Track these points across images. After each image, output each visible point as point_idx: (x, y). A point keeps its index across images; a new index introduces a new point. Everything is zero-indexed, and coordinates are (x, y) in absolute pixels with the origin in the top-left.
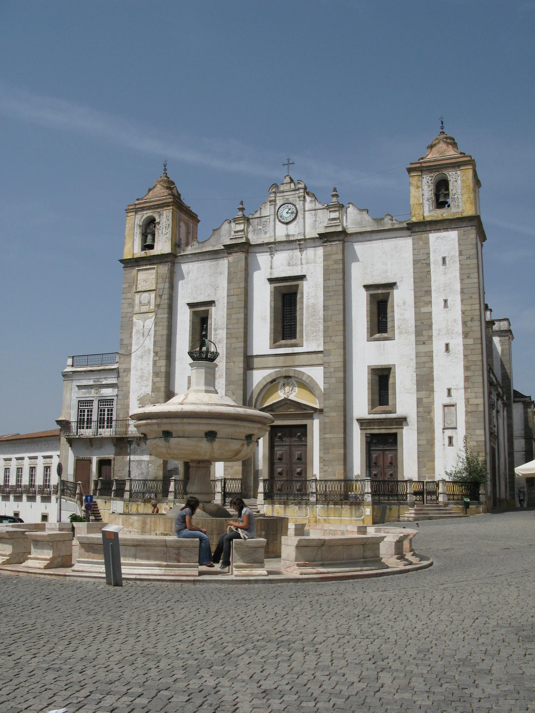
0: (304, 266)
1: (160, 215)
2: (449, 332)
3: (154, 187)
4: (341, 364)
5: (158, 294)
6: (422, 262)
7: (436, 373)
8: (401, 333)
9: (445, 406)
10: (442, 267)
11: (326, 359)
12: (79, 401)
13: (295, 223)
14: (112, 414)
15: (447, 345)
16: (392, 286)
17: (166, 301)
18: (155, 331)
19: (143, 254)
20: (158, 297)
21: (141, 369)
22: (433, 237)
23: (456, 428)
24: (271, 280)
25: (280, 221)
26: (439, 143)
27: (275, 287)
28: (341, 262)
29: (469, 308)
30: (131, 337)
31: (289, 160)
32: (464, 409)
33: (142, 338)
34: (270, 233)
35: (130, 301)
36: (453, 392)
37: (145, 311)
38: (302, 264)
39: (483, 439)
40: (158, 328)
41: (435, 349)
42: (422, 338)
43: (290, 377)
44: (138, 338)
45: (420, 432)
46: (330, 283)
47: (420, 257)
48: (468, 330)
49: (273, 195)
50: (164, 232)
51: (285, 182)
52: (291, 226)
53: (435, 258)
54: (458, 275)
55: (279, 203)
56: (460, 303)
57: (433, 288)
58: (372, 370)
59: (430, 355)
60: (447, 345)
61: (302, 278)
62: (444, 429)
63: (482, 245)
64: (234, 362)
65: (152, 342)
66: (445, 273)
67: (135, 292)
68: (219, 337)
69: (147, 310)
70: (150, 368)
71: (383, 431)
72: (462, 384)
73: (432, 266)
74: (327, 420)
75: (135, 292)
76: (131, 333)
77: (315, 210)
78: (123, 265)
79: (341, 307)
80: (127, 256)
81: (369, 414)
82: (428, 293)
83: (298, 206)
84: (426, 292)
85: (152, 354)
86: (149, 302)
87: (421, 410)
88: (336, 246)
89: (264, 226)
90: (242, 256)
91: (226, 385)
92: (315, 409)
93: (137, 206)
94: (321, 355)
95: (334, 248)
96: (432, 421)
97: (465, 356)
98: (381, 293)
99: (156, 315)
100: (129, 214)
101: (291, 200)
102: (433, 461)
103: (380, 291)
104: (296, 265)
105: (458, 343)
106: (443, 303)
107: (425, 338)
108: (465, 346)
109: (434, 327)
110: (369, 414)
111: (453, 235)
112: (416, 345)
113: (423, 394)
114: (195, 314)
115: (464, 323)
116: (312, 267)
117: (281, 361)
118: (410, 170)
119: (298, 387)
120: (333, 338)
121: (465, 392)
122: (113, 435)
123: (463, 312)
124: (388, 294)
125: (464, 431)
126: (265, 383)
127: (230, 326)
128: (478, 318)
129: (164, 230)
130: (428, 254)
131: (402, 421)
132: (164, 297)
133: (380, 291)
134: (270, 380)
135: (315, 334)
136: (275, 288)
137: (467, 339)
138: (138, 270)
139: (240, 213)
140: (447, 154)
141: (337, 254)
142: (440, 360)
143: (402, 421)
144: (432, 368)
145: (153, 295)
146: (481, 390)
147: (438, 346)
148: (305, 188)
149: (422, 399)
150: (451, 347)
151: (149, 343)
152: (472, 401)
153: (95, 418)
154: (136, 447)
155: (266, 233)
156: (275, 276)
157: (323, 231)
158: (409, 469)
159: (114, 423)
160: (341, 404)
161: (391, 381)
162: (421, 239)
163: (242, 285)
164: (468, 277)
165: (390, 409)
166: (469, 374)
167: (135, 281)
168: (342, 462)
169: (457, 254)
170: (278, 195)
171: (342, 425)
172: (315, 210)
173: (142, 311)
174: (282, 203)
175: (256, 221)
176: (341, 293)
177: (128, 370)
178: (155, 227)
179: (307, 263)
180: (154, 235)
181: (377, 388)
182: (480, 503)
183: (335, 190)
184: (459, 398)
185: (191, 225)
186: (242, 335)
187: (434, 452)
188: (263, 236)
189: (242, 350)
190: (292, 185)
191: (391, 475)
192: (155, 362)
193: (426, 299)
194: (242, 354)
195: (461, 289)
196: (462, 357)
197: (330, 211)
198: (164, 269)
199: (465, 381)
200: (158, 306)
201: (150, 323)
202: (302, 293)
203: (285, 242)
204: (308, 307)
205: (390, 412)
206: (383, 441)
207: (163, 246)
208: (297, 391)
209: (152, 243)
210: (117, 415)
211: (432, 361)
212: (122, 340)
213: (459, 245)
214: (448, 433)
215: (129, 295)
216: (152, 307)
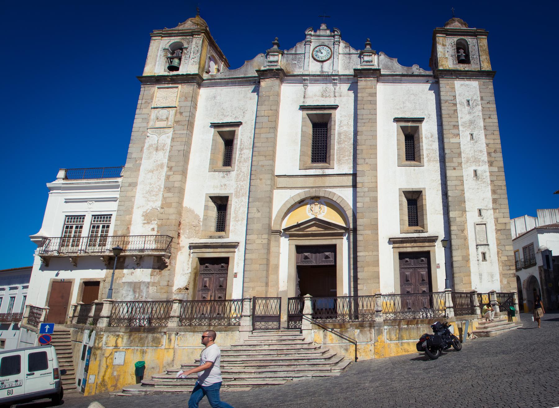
2: (476, 160)
5: (179, 111)
6: (450, 102)
7: (467, 195)
10: (466, 107)
15: (475, 171)
16: (420, 120)
29: (492, 142)
36: (483, 213)
41: (465, 174)
48: (493, 159)
54: (481, 114)
56: (484, 137)
57: (460, 123)
59: (461, 179)
60: (475, 171)
67: (152, 108)
69: (165, 126)
71: (416, 250)
72: (491, 205)
73: (458, 106)
75: (152, 108)
82: (456, 127)
84: (454, 126)
86: (167, 118)
98: (411, 126)
99: (174, 131)
103: (410, 124)
105: (484, 169)
106: (469, 136)
109: (463, 155)
111: (474, 84)
115: (489, 154)
117: (310, 182)
121: (494, 213)
123: (487, 145)
124: (417, 129)
126: (293, 203)
130: (455, 97)
132: (184, 114)
133: (410, 124)
135: (347, 158)
137: (492, 168)
138: (159, 88)
142: (469, 183)
144: (463, 190)
145: (172, 112)
147: (467, 172)
150: (478, 173)
152: (501, 220)
162: (448, 84)
164: (489, 118)
166: (496, 196)
169: (479, 99)
184: (489, 217)
193: (455, 131)
195: (484, 126)
196: (489, 182)
199: (493, 203)
200: (177, 122)
201: (166, 138)
204: (340, 134)
208: (326, 212)
211: (463, 184)
213: (480, 92)
215: (145, 111)
216: (170, 123)
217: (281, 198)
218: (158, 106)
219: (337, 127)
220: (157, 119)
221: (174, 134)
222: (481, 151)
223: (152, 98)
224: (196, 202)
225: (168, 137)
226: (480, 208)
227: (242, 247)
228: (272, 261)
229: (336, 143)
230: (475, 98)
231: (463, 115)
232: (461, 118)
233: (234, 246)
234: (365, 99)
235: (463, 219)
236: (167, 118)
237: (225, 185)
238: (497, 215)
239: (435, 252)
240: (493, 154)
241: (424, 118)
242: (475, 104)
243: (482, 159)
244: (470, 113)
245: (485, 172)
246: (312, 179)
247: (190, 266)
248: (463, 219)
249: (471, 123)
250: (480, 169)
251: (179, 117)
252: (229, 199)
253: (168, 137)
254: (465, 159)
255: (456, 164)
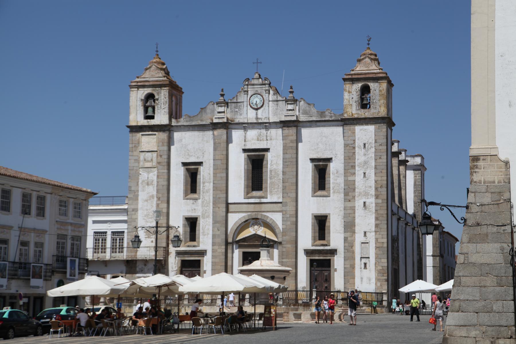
0: (269, 142)
1: (158, 94)
2: (366, 194)
3: (150, 67)
4: (294, 212)
7: (357, 221)
8: (334, 192)
9: (362, 243)
10: (363, 150)
11: (284, 208)
12: (94, 232)
13: (262, 109)
14: (123, 242)
16: (329, 160)
17: (166, 160)
18: (158, 182)
19: (145, 122)
20: (159, 156)
21: (147, 210)
22: (358, 129)
23: (369, 258)
24: (245, 151)
25: (251, 107)
26: (365, 58)
27: (248, 155)
28: (295, 142)
29: (379, 179)
30: (138, 185)
31: (257, 60)
32: (374, 245)
33: (147, 186)
34: (244, 115)
35: (136, 158)
36: (367, 234)
37: (149, 166)
38: (267, 140)
39: (386, 265)
40: (160, 180)
42: (349, 198)
43: (258, 219)
44: (144, 187)
45: (345, 259)
46: (287, 156)
47: (349, 142)
48: (379, 193)
49: (246, 87)
50: (162, 107)
51: (255, 77)
52: (260, 111)
53: (359, 143)
54: (373, 156)
55: (250, 93)
58: (315, 216)
59: (353, 209)
60: (365, 203)
61: (267, 150)
62: (361, 258)
63: (392, 130)
64: (219, 208)
65: (155, 190)
66: (365, 155)
68: (206, 188)
69: (151, 166)
70: (155, 209)
71: (321, 258)
72: (373, 229)
73: (357, 149)
74: (284, 250)
76: (138, 182)
77: (277, 101)
78: (129, 129)
79: (295, 173)
80: (133, 123)
81: (312, 246)
82: (353, 167)
83: (264, 97)
84: (352, 166)
85: (155, 199)
86: (152, 160)
87: (347, 244)
88: (292, 131)
89: (240, 109)
90: (224, 131)
91: (213, 224)
92: (275, 242)
93: (139, 84)
94: (280, 205)
95: (291, 131)
96: (353, 252)
97: (376, 210)
98: (322, 165)
100: (132, 89)
101: (259, 92)
102: (354, 278)
104: (263, 140)
105: (371, 201)
106: (363, 174)
107: (351, 197)
108: (376, 204)
109: (357, 190)
110: (312, 246)
111: (371, 128)
112: (344, 201)
113: (348, 234)
114: (188, 170)
115: (376, 189)
116: (274, 142)
117: (251, 208)
118: (345, 80)
119: (264, 227)
120: (289, 194)
121: (375, 234)
122: (125, 258)
123: (376, 182)
124: (326, 166)
125: (374, 259)
127: (215, 182)
128: (386, 186)
129: (162, 105)
131: (333, 252)
132: (163, 156)
134: (244, 220)
135: (276, 190)
136: (248, 155)
138: (142, 135)
139: (222, 98)
140: (370, 68)
141: (292, 135)
143: (333, 252)
144: (355, 217)
145: (155, 154)
146: (386, 233)
147: (359, 204)
148: (270, 84)
149: (347, 238)
150: (367, 204)
151: (152, 190)
152: (379, 240)
153: (109, 244)
154: (144, 266)
155: (241, 115)
156: (247, 147)
157: (283, 119)
158: (338, 283)
159: (125, 250)
160: (295, 239)
161: (327, 224)
162: (350, 130)
163: (225, 153)
164: (380, 158)
165: (326, 243)
166: (378, 222)
167: (139, 142)
168: (294, 278)
169: (374, 141)
170: (249, 87)
171: (295, 253)
172: (277, 101)
173: (146, 166)
174: (253, 93)
175: (233, 105)
176: (295, 163)
177: (136, 210)
178: (154, 101)
179: (271, 139)
180: (154, 108)
181: (317, 228)
182: (383, 307)
183: (291, 88)
184: (372, 238)
185: (179, 97)
186: (225, 188)
187: (354, 272)
188: (239, 117)
189: (225, 200)
190: (260, 80)
191: (326, 287)
192: (158, 205)
193: (352, 171)
194: (225, 202)
195: (375, 166)
196: (374, 211)
197: (288, 104)
198: (163, 136)
199: (375, 227)
200: (159, 163)
201: (153, 175)
202: (267, 161)
203: (255, 123)
204: (271, 171)
205: (326, 245)
206: (321, 264)
207: (161, 117)
209: (153, 115)
210: (128, 243)
211: (354, 213)
212: (130, 187)
213: (375, 135)
214: (364, 261)
215: (135, 153)
216: (154, 164)
217: (234, 219)
218: (144, 150)
219: (269, 166)
220: (145, 160)
221: (158, 172)
222: (370, 187)
223: (139, 143)
224: (177, 222)
225: (154, 175)
226: (366, 230)
227: (209, 254)
228: (229, 263)
229: (268, 179)
230: (370, 141)
231: (360, 156)
232: (358, 159)
233: (203, 253)
234: (288, 145)
235: (352, 238)
236: (152, 160)
237: (195, 209)
238: (378, 236)
239: (334, 260)
240: (379, 189)
241: (331, 159)
242: (370, 147)
243: (371, 193)
244: (365, 155)
245: (372, 203)
246: (252, 205)
247: (176, 265)
248: (352, 238)
249: (365, 163)
250: (368, 201)
251: (160, 159)
252: (198, 219)
253: (154, 175)
254: (358, 193)
255: (351, 197)
